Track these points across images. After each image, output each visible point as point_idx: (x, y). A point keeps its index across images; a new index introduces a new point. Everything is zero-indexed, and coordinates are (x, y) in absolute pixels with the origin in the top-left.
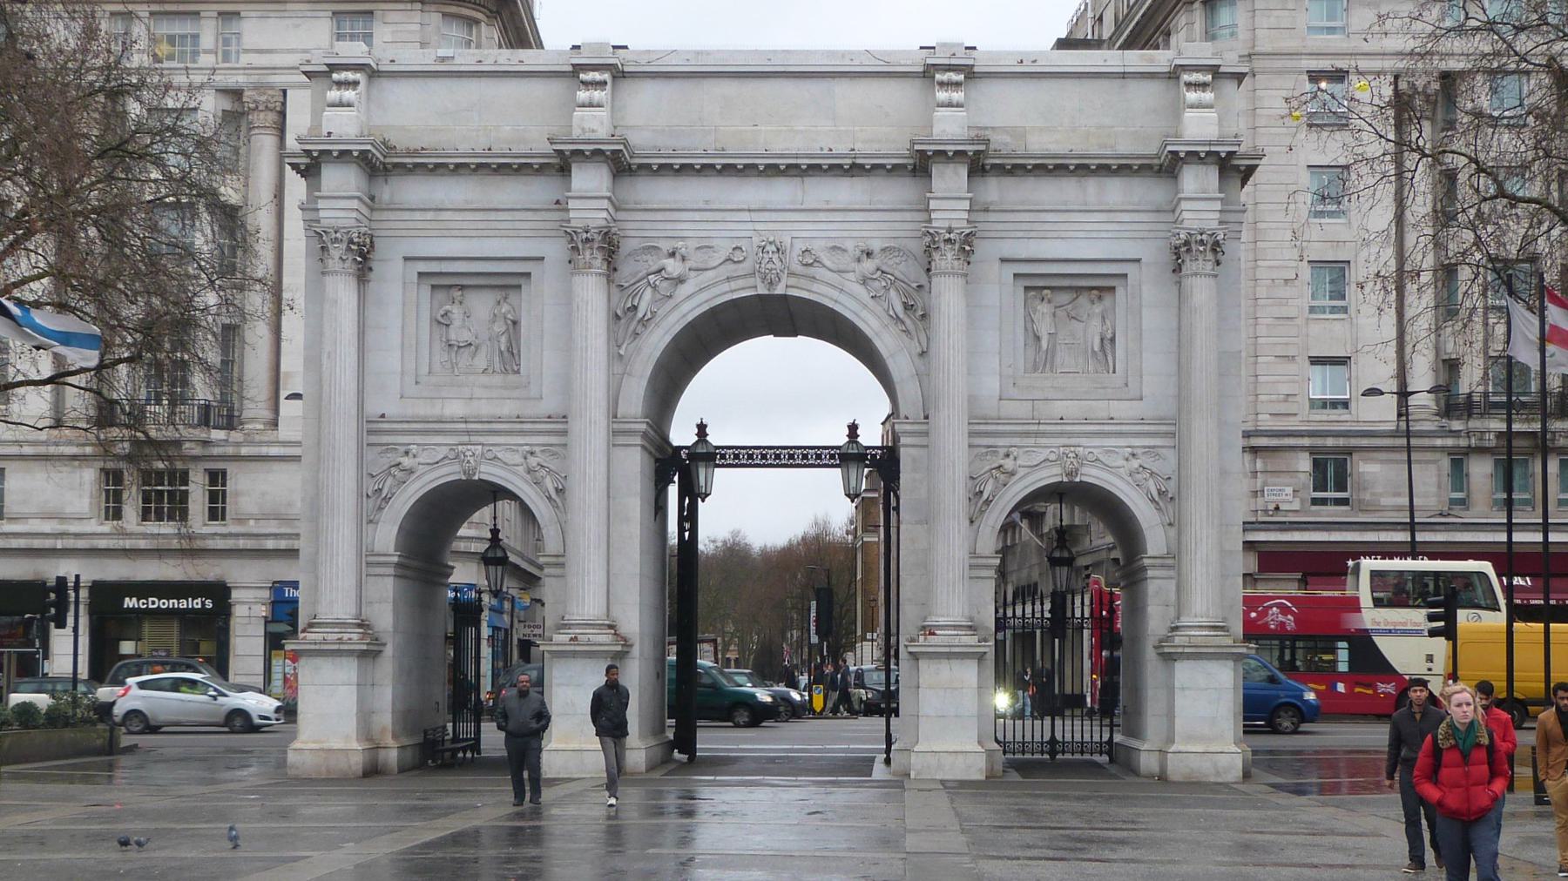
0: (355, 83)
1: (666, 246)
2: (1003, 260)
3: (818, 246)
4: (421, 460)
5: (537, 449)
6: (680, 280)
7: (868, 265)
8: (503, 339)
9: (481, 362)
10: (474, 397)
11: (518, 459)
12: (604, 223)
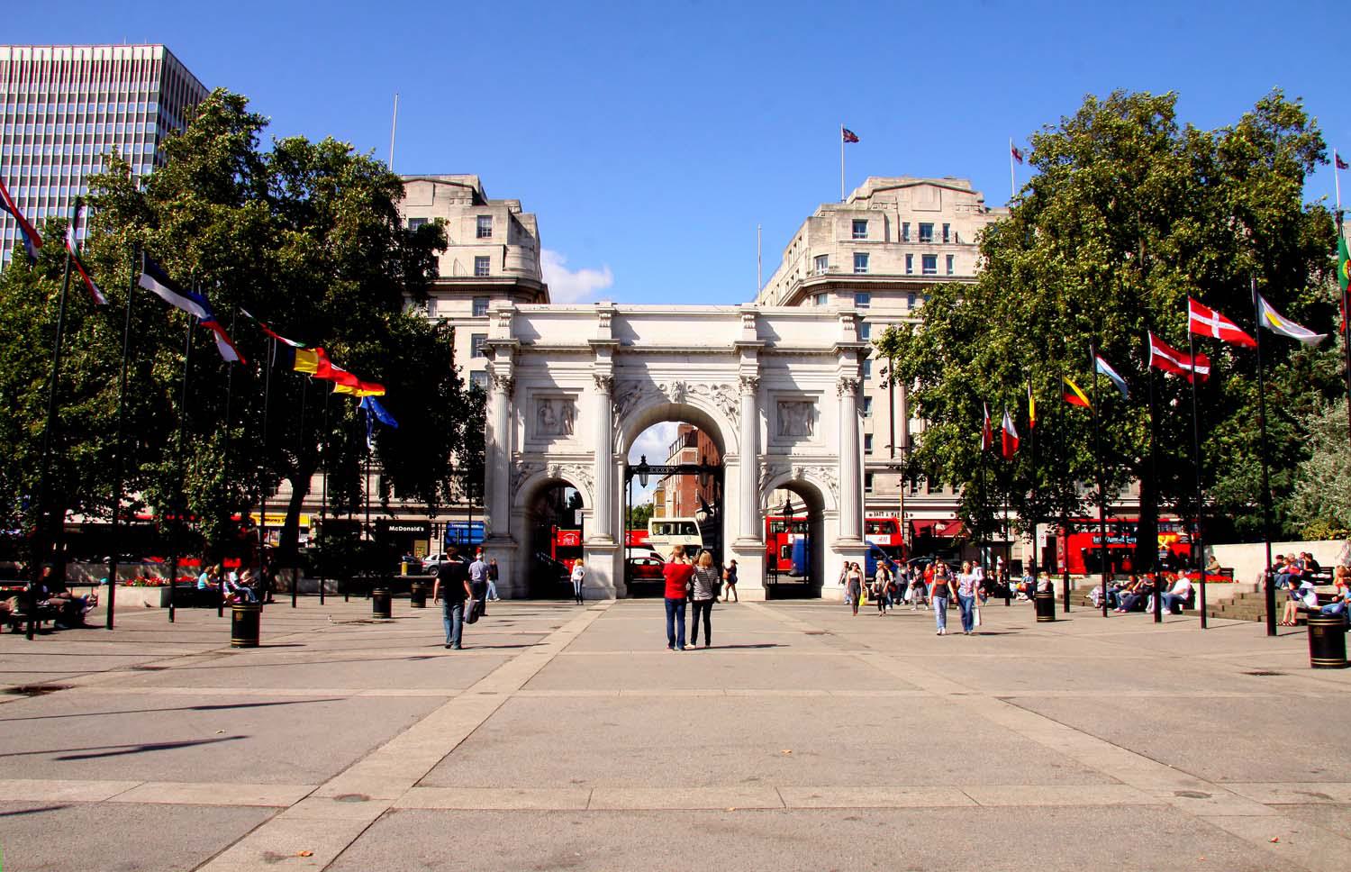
0: (508, 318)
1: (633, 383)
2: (769, 390)
3: (694, 385)
6: (640, 398)
7: (716, 392)
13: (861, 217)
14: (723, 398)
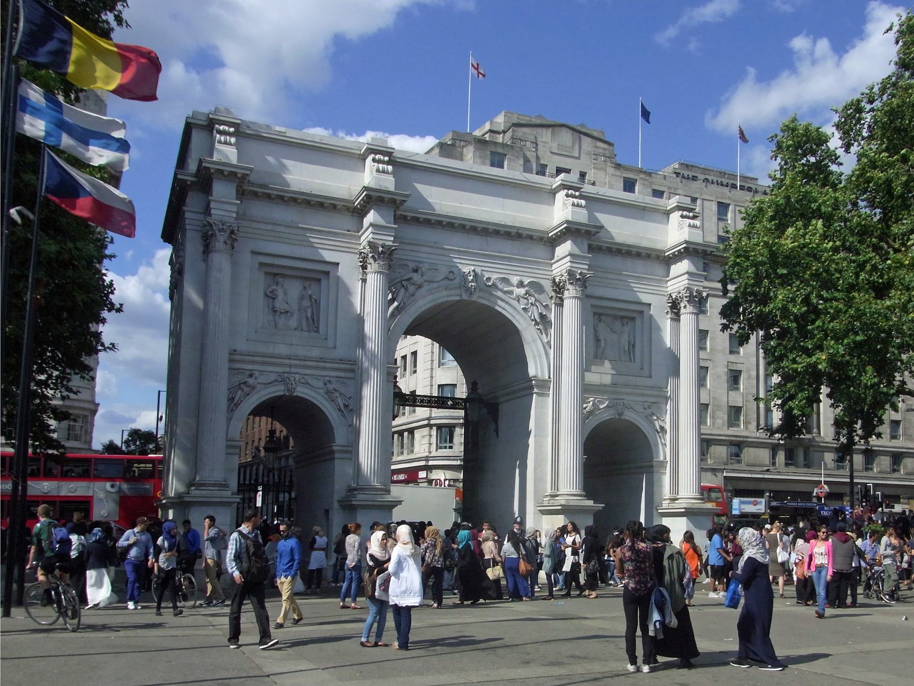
1: (412, 265)
3: (494, 277)
4: (259, 381)
5: (333, 379)
6: (420, 287)
7: (522, 291)
8: (309, 311)
9: (293, 323)
10: (291, 344)
11: (320, 384)
12: (391, 244)
13: (500, 150)
14: (532, 300)
